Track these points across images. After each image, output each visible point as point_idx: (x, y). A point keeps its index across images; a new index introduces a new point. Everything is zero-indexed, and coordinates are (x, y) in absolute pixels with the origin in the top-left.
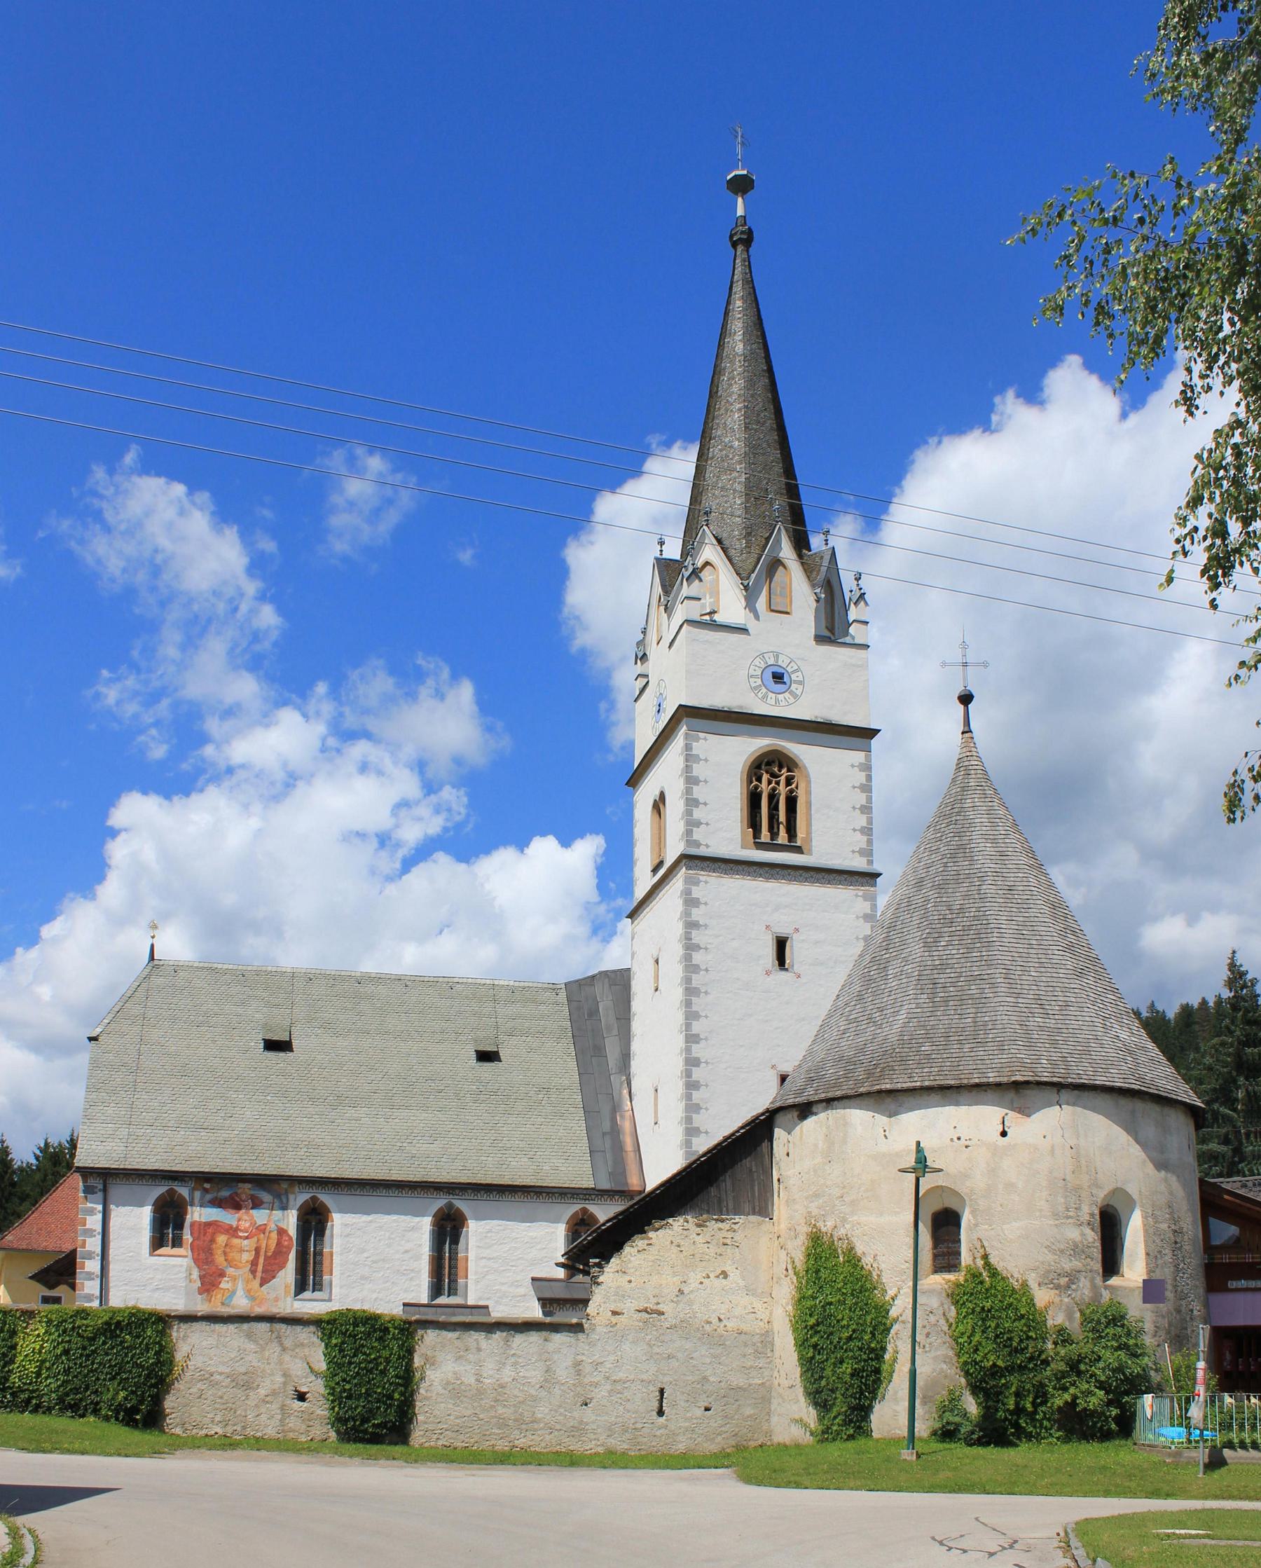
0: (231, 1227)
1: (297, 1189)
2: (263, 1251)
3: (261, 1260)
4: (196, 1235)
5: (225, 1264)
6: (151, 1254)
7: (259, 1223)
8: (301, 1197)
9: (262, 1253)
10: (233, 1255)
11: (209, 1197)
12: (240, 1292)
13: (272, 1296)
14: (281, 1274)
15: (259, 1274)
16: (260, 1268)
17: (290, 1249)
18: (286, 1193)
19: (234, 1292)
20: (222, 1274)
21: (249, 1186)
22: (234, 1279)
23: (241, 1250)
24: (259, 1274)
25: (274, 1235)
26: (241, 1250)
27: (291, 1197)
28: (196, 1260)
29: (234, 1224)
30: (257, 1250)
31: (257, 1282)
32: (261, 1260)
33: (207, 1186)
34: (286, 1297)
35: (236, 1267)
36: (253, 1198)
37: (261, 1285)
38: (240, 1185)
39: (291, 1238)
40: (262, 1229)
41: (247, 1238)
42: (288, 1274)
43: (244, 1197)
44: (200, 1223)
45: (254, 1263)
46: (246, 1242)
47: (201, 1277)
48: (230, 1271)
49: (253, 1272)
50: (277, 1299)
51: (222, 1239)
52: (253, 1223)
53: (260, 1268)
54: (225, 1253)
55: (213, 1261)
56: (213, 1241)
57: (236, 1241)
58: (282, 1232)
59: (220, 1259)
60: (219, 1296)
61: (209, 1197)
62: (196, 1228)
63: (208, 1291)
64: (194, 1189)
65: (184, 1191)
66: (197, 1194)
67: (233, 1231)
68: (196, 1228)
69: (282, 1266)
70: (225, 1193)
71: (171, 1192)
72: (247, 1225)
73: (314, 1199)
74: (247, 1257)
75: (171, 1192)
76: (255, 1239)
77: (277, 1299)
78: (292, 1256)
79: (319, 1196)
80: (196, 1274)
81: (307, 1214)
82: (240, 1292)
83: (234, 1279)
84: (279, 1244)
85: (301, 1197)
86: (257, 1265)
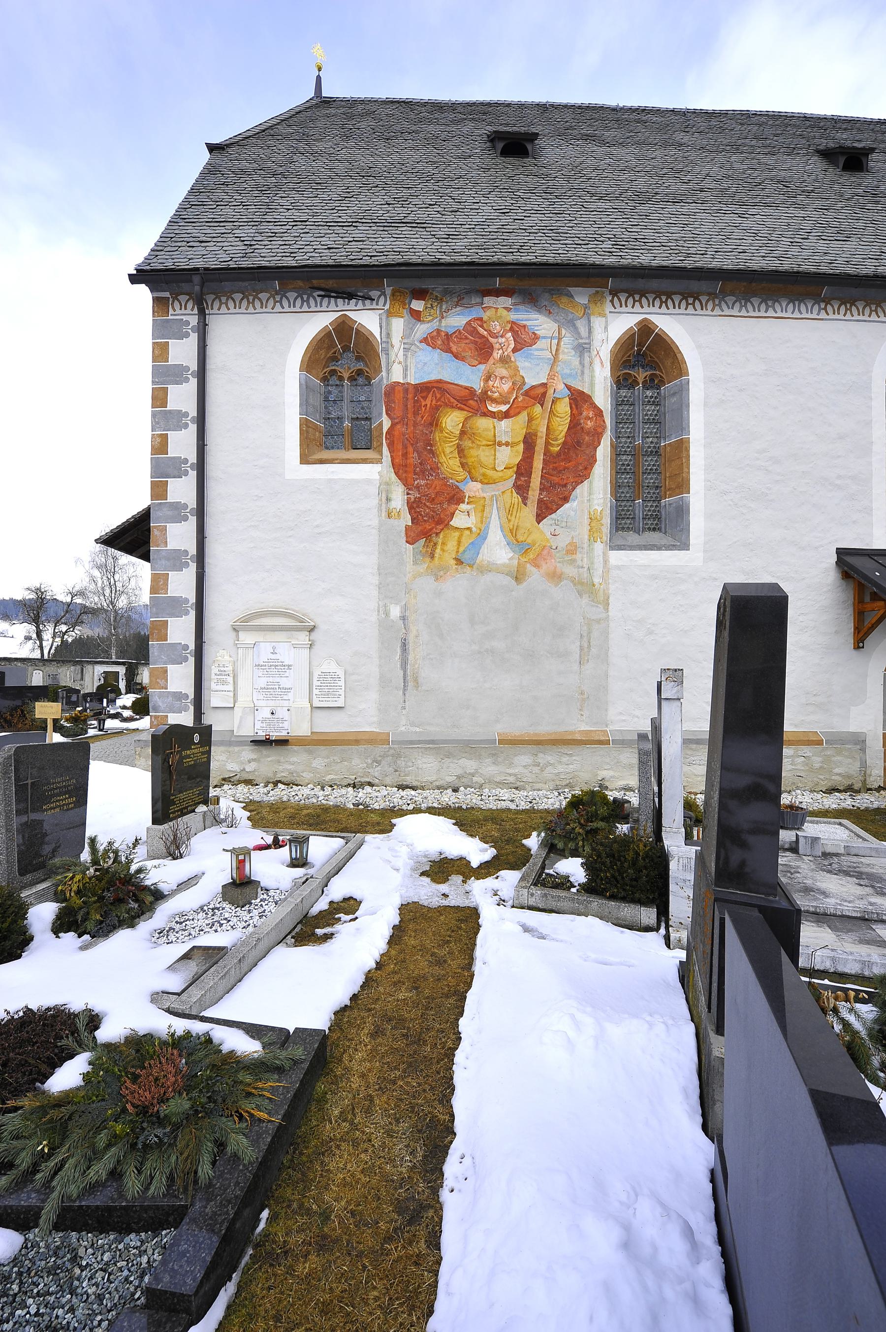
0: (471, 391)
1: (608, 307)
4: (398, 413)
5: (462, 474)
6: (305, 459)
7: (532, 380)
8: (614, 324)
10: (480, 454)
11: (423, 329)
12: (495, 534)
13: (562, 541)
14: (581, 491)
17: (597, 435)
18: (587, 315)
19: (482, 536)
20: (457, 497)
21: (505, 301)
22: (482, 507)
25: (564, 408)
28: (400, 469)
29: (478, 386)
30: (529, 442)
31: (529, 513)
33: (418, 305)
34: (592, 539)
35: (486, 481)
36: (516, 329)
37: (540, 518)
38: (488, 301)
39: (599, 413)
40: (538, 395)
41: (506, 415)
42: (595, 493)
43: (496, 327)
44: (406, 388)
45: (523, 470)
46: (504, 424)
47: (412, 506)
48: (472, 488)
49: (522, 489)
50: (572, 549)
51: (452, 420)
52: (518, 384)
54: (461, 451)
55: (436, 468)
56: (434, 423)
57: (483, 424)
59: (450, 463)
60: (451, 545)
61: (423, 329)
62: (399, 395)
63: (427, 535)
64: (389, 314)
65: (367, 319)
66: (398, 325)
67: (473, 402)
68: (399, 395)
69: (583, 473)
70: (456, 320)
72: (506, 387)
73: (645, 329)
74: (508, 457)
76: (523, 417)
77: (572, 549)
78: (603, 451)
79: (654, 319)
80: (399, 497)
81: (627, 364)
82: (495, 534)
83: (482, 507)
84: (574, 425)
85: (614, 324)
86: (529, 474)
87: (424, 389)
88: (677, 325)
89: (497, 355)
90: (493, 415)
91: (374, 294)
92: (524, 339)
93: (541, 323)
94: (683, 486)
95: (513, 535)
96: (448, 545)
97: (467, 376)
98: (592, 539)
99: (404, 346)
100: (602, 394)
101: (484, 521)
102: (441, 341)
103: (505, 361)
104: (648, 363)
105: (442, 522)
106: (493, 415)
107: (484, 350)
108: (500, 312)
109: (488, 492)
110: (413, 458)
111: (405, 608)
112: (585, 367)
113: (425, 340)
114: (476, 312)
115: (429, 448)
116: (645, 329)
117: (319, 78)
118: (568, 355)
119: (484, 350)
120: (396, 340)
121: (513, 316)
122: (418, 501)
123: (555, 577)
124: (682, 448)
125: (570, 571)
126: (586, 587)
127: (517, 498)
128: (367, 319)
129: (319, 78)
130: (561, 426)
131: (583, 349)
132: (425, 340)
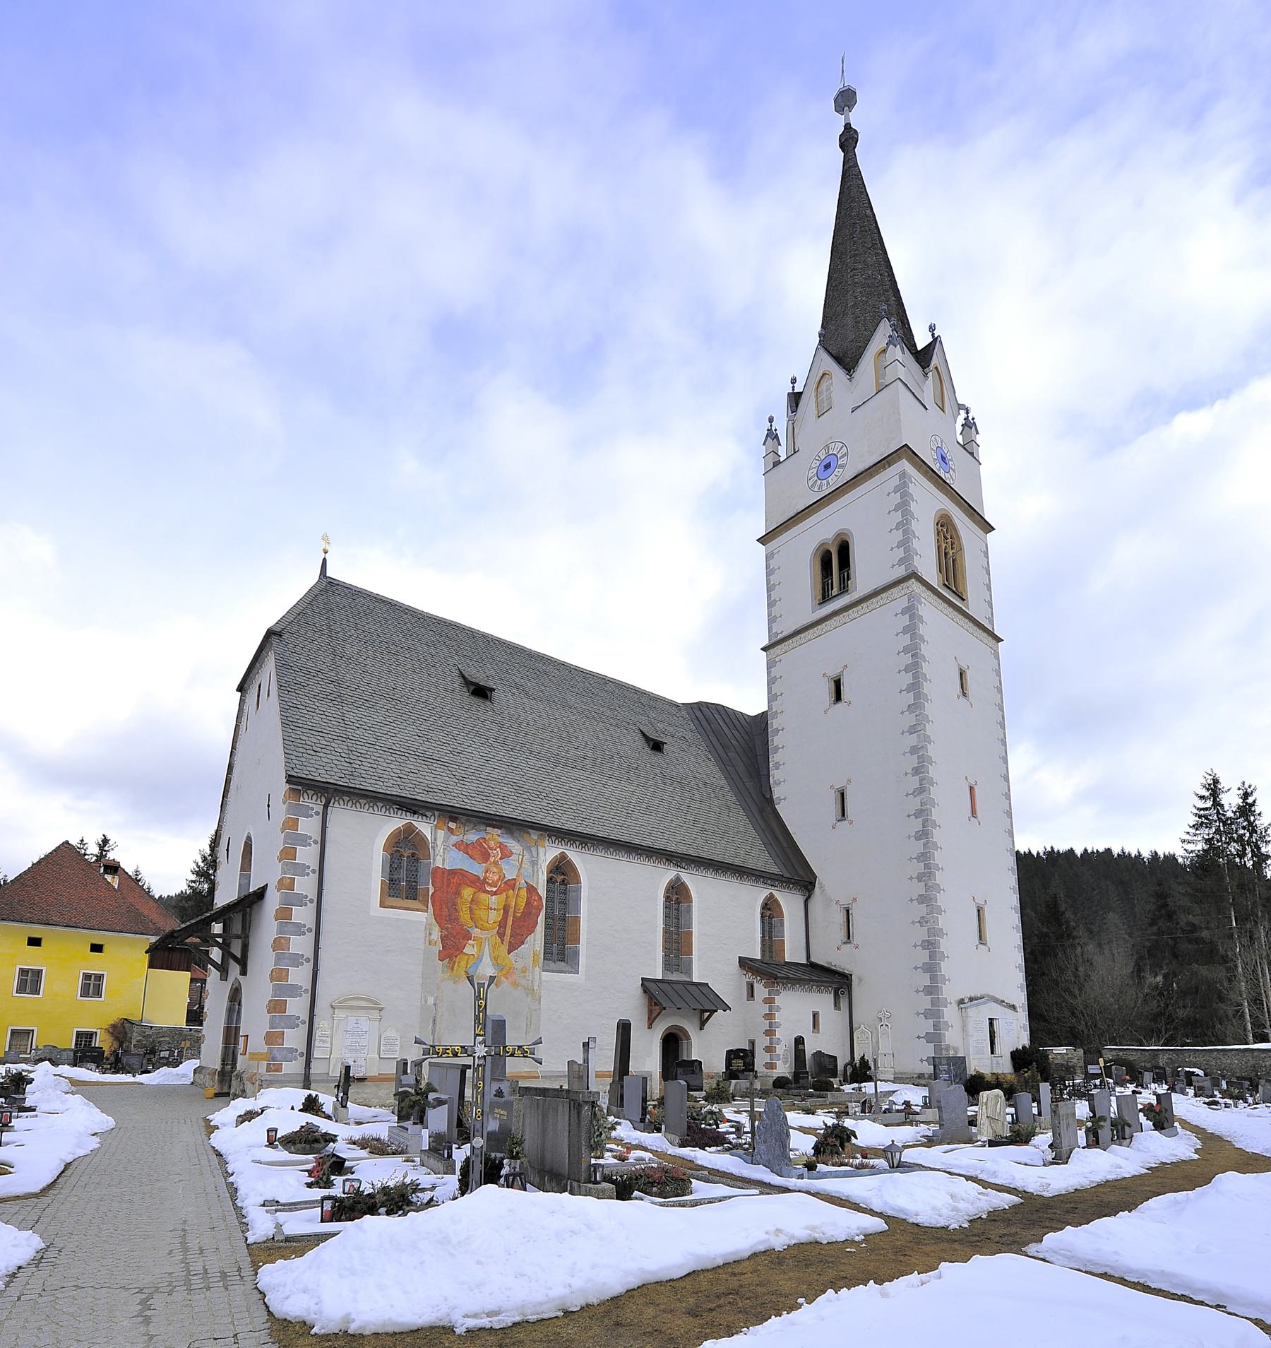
2: (512, 910)
3: (510, 922)
7: (508, 877)
9: (511, 913)
10: (481, 914)
11: (454, 839)
12: (487, 959)
13: (519, 966)
15: (507, 938)
16: (508, 931)
18: (536, 845)
20: (468, 937)
23: (489, 908)
24: (507, 938)
25: (524, 893)
26: (489, 908)
27: (541, 850)
28: (437, 916)
29: (482, 876)
30: (506, 909)
31: (505, 947)
32: (510, 922)
34: (534, 966)
36: (502, 846)
37: (509, 952)
40: (511, 884)
41: (495, 893)
42: (536, 940)
43: (492, 844)
45: (502, 925)
48: (476, 932)
49: (501, 935)
50: (524, 970)
51: (467, 893)
52: (502, 877)
53: (508, 931)
54: (471, 910)
55: (457, 919)
56: (458, 893)
57: (483, 896)
58: (531, 889)
59: (465, 916)
60: (463, 964)
61: (454, 839)
63: (450, 957)
65: (425, 827)
66: (441, 834)
67: (478, 884)
69: (531, 930)
70: (472, 837)
71: (409, 829)
72: (496, 878)
73: (563, 856)
74: (495, 916)
75: (409, 829)
77: (524, 970)
78: (541, 919)
80: (436, 934)
82: (487, 959)
84: (528, 903)
85: (549, 852)
87: (453, 872)
88: (577, 857)
89: (492, 859)
90: (488, 892)
91: (428, 814)
92: (506, 854)
93: (514, 846)
94: (577, 941)
95: (495, 959)
96: (461, 963)
97: (477, 869)
98: (534, 966)
99: (443, 848)
100: (542, 891)
101: (481, 951)
102: (462, 847)
103: (496, 863)
104: (562, 873)
105: (460, 950)
106: (488, 892)
107: (485, 856)
108: (495, 836)
109: (484, 935)
110: (445, 912)
111: (436, 999)
112: (535, 873)
113: (454, 845)
114: (482, 834)
115: (454, 907)
116: (563, 856)
117: (324, 560)
118: (527, 865)
119: (485, 856)
120: (439, 842)
121: (501, 840)
122: (446, 936)
123: (515, 985)
124: (577, 919)
125: (523, 982)
126: (530, 991)
127: (498, 940)
128: (425, 827)
129: (324, 560)
130: (522, 904)
131: (534, 863)
132: (454, 845)
